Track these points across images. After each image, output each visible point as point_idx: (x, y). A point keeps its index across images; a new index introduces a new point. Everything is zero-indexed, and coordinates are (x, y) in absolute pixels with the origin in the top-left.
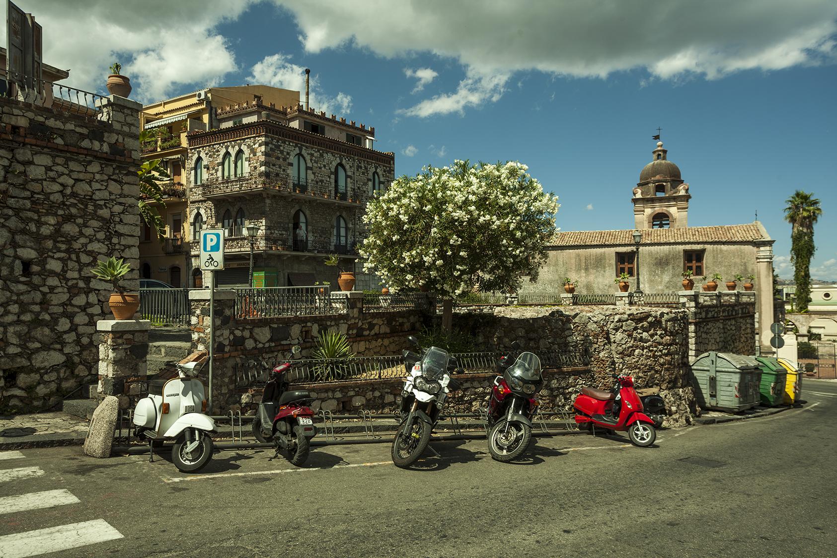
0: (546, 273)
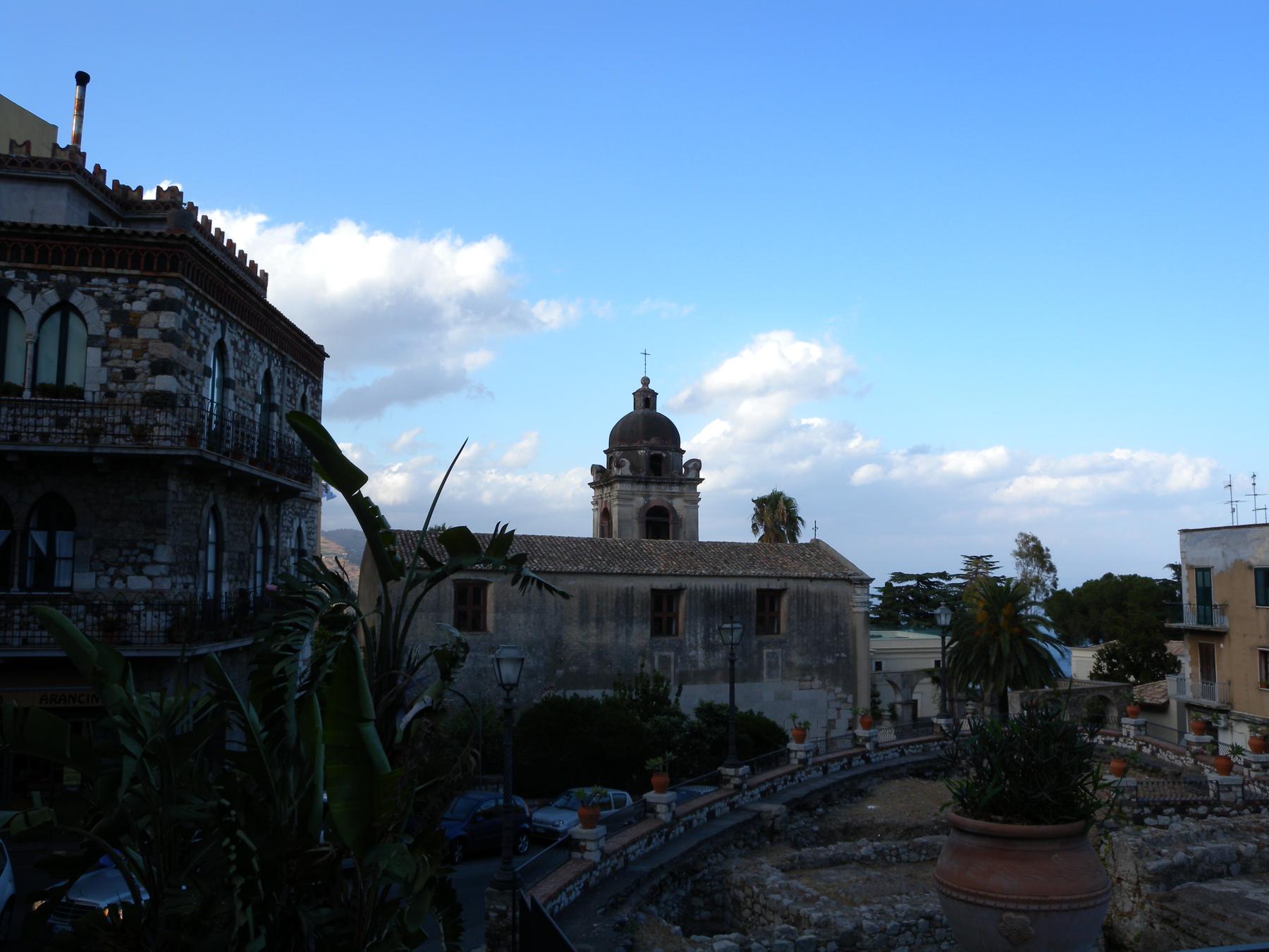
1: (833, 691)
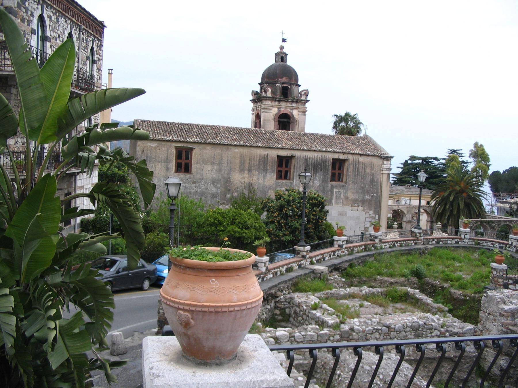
0: (210, 172)
1: (369, 213)
